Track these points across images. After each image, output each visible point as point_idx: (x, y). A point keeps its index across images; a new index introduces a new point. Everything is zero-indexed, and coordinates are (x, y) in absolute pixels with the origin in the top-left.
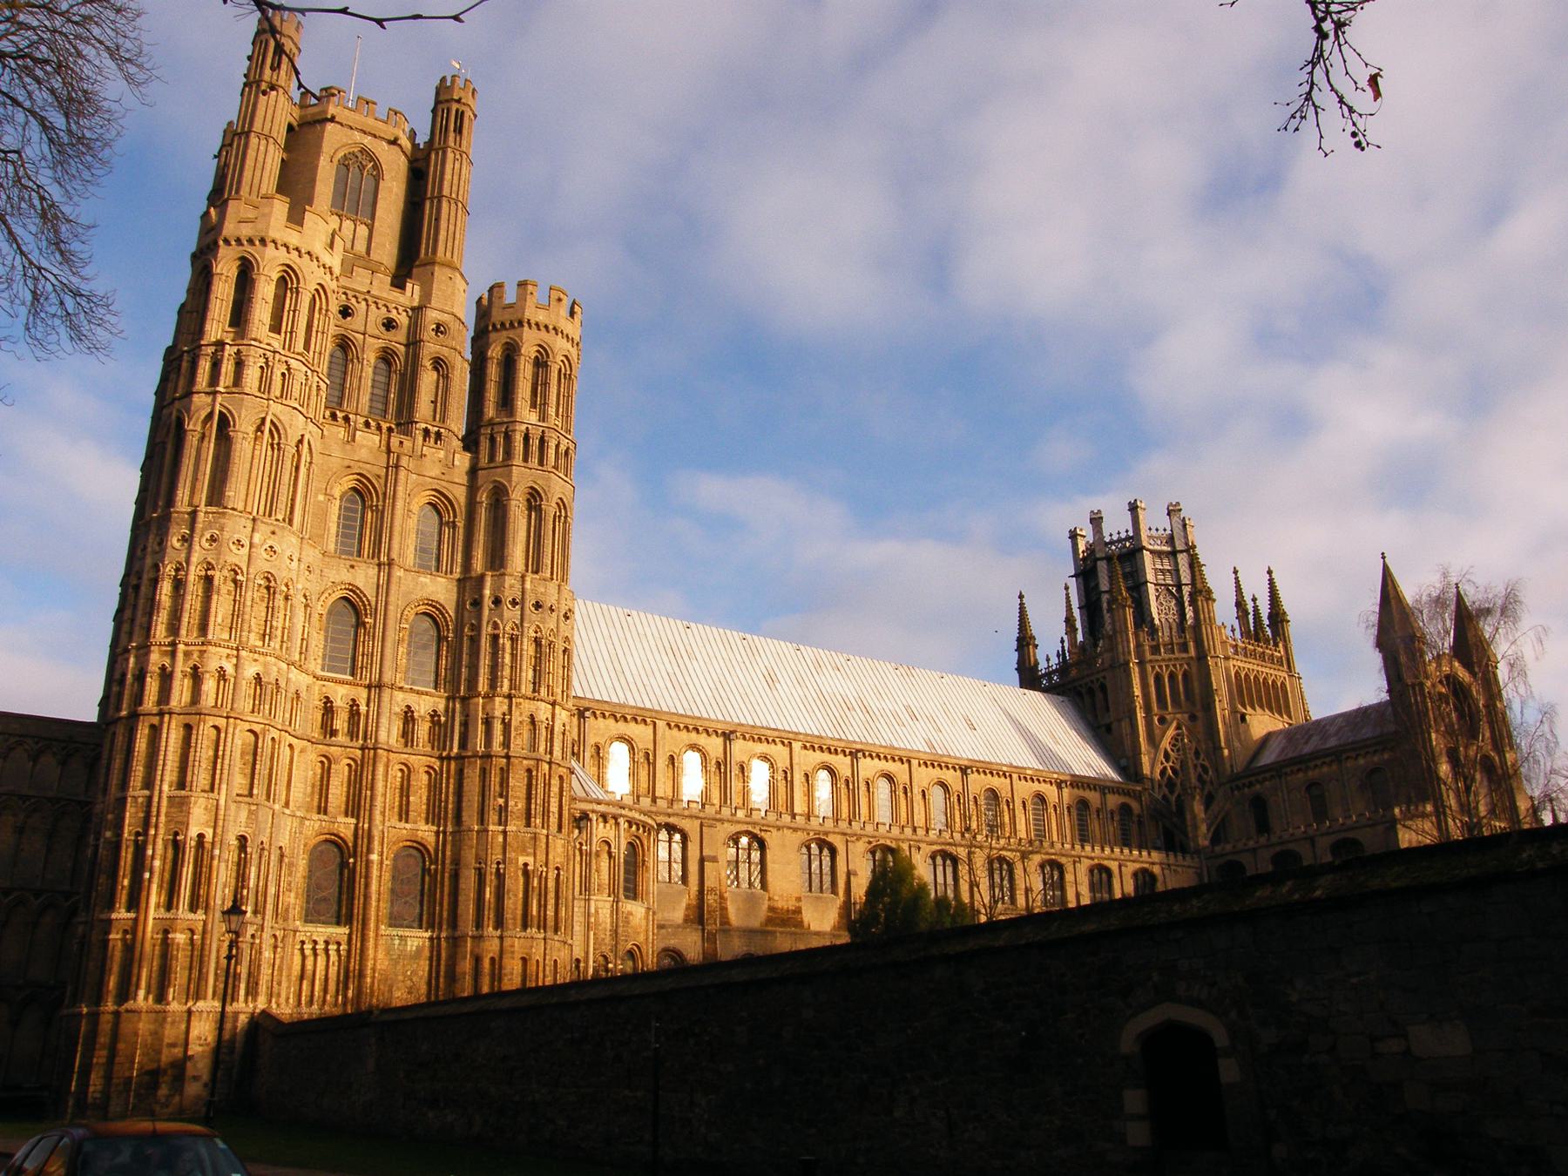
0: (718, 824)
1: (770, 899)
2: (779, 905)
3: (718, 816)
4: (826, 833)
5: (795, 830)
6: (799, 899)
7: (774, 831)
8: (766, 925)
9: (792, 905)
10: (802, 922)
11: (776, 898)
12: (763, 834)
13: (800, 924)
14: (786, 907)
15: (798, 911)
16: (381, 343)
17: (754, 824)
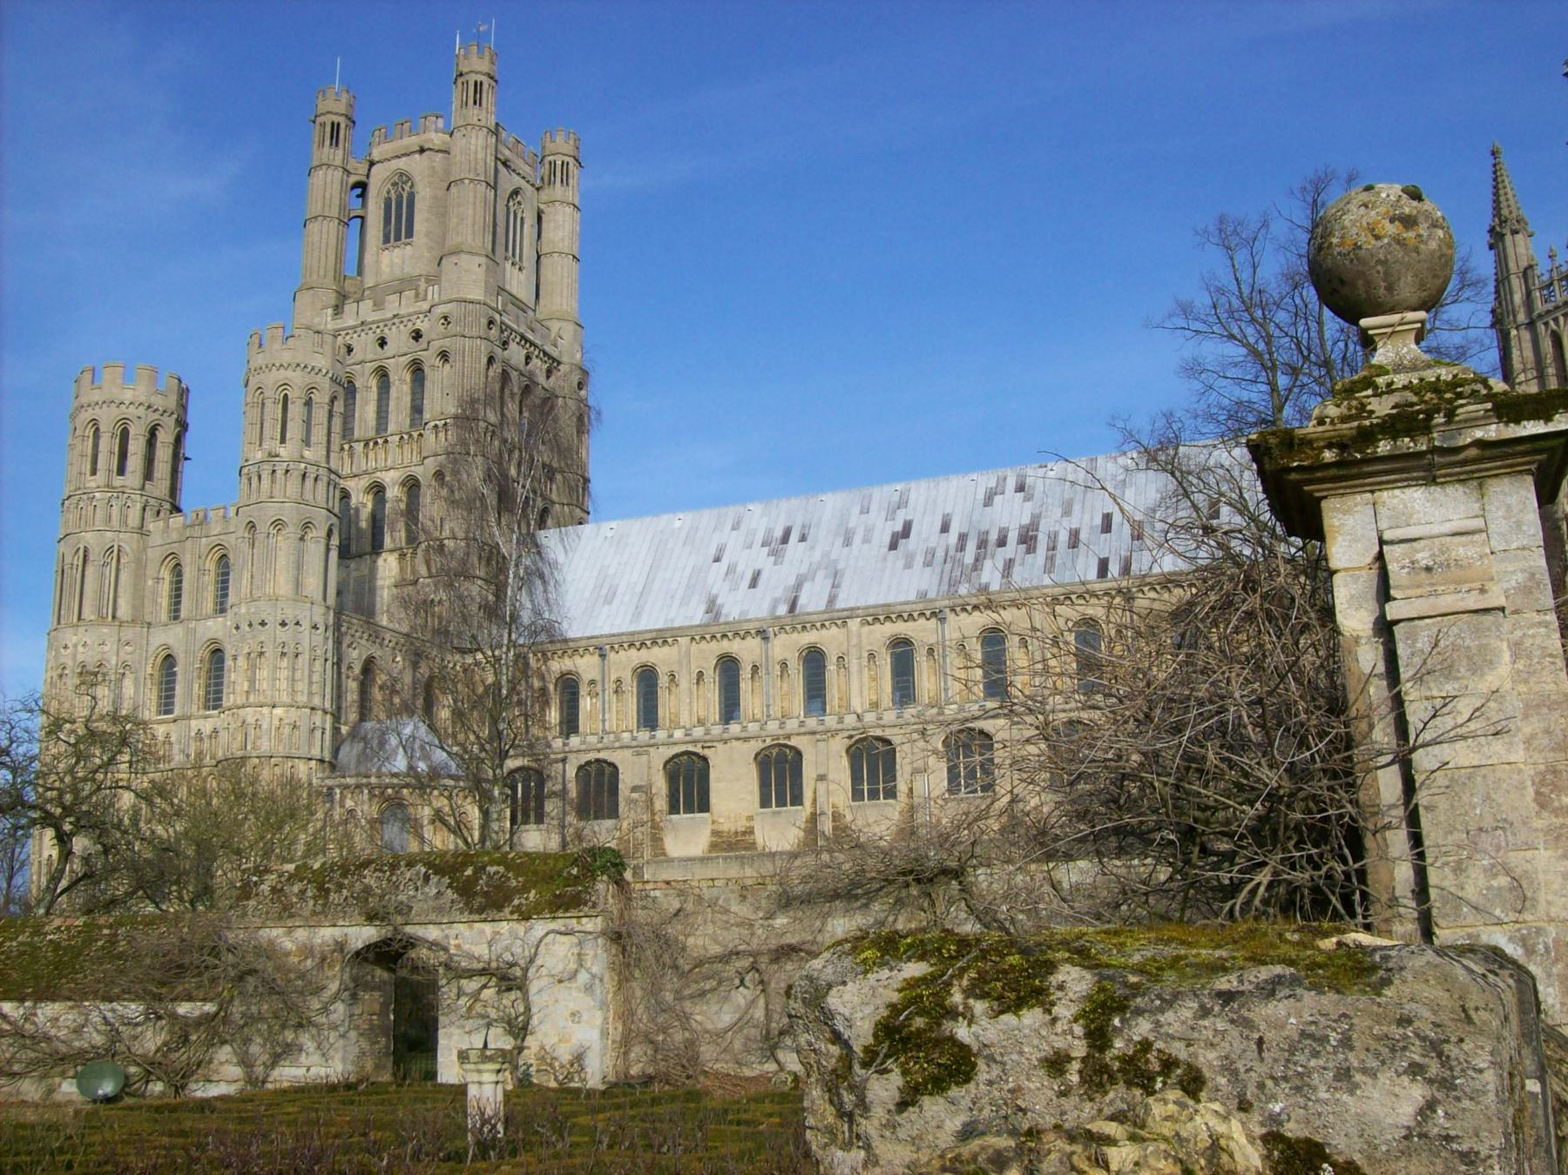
0: (651, 750)
1: (713, 822)
2: (727, 826)
3: (652, 741)
4: (788, 737)
5: (746, 739)
6: (750, 818)
7: (720, 746)
8: (710, 851)
9: (741, 825)
10: (754, 843)
11: (721, 820)
12: (706, 752)
13: (753, 845)
14: (733, 829)
15: (750, 831)
16: (409, 358)
17: (695, 742)
